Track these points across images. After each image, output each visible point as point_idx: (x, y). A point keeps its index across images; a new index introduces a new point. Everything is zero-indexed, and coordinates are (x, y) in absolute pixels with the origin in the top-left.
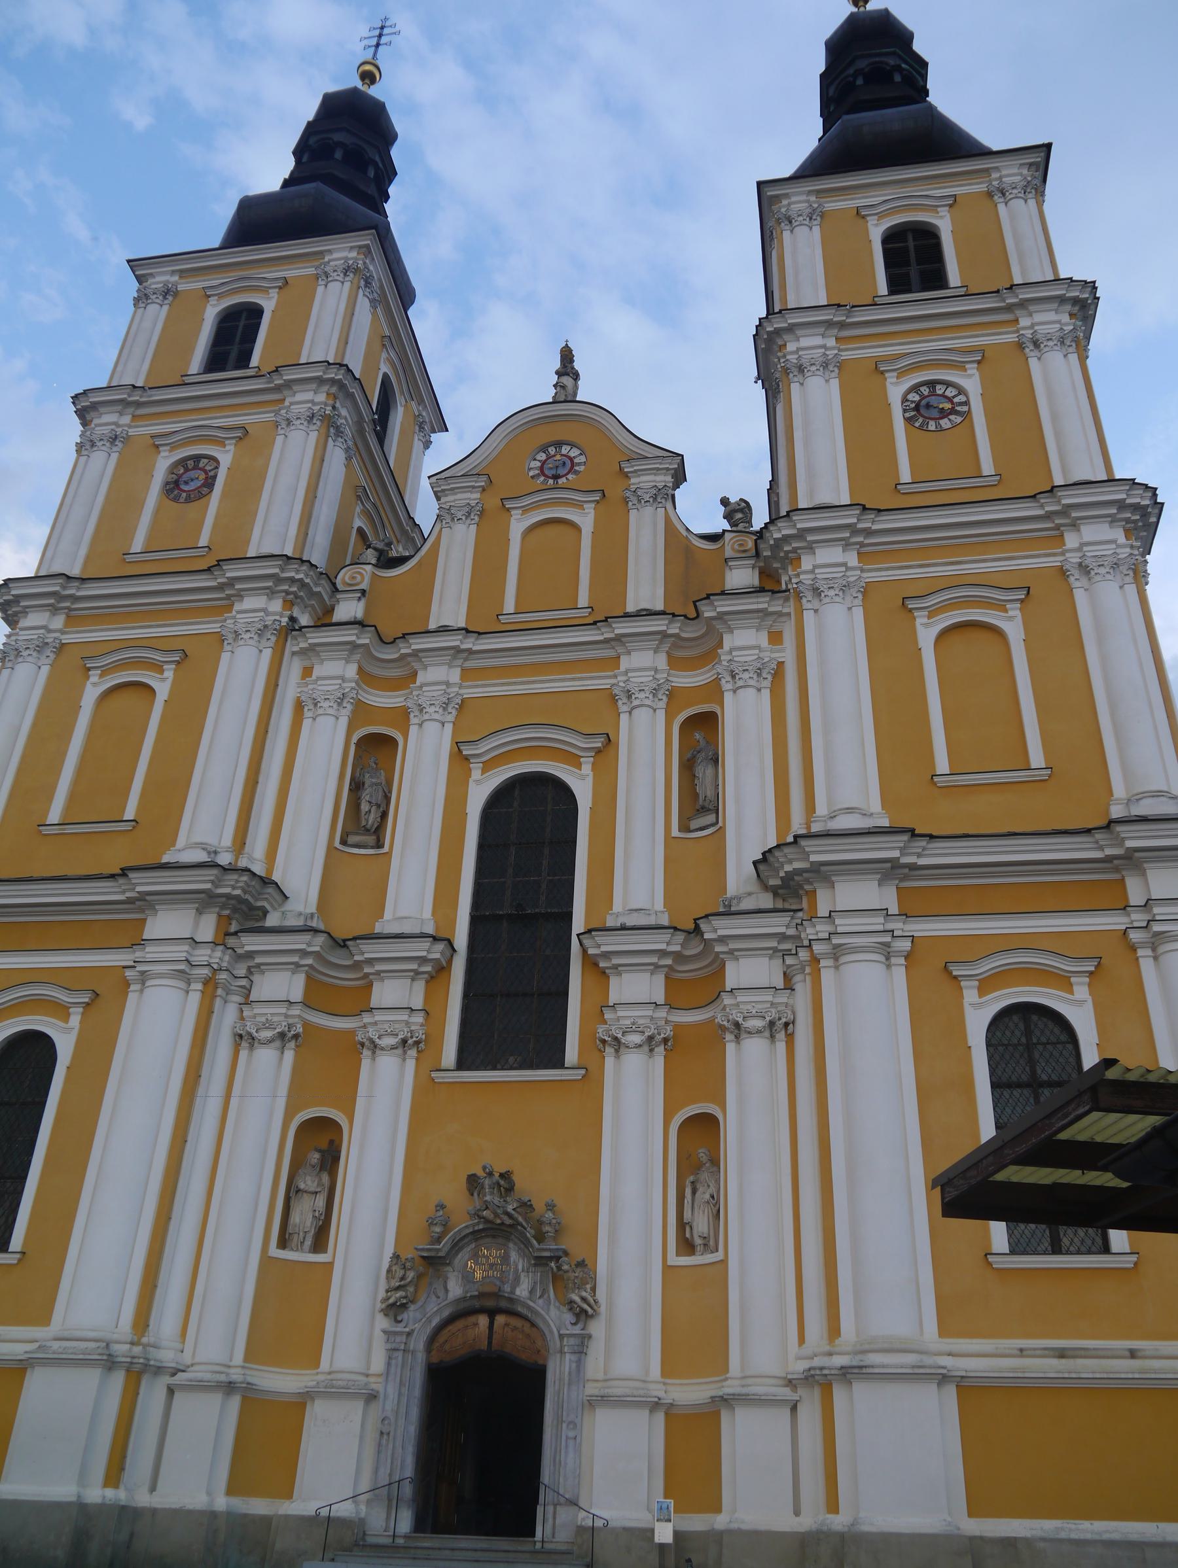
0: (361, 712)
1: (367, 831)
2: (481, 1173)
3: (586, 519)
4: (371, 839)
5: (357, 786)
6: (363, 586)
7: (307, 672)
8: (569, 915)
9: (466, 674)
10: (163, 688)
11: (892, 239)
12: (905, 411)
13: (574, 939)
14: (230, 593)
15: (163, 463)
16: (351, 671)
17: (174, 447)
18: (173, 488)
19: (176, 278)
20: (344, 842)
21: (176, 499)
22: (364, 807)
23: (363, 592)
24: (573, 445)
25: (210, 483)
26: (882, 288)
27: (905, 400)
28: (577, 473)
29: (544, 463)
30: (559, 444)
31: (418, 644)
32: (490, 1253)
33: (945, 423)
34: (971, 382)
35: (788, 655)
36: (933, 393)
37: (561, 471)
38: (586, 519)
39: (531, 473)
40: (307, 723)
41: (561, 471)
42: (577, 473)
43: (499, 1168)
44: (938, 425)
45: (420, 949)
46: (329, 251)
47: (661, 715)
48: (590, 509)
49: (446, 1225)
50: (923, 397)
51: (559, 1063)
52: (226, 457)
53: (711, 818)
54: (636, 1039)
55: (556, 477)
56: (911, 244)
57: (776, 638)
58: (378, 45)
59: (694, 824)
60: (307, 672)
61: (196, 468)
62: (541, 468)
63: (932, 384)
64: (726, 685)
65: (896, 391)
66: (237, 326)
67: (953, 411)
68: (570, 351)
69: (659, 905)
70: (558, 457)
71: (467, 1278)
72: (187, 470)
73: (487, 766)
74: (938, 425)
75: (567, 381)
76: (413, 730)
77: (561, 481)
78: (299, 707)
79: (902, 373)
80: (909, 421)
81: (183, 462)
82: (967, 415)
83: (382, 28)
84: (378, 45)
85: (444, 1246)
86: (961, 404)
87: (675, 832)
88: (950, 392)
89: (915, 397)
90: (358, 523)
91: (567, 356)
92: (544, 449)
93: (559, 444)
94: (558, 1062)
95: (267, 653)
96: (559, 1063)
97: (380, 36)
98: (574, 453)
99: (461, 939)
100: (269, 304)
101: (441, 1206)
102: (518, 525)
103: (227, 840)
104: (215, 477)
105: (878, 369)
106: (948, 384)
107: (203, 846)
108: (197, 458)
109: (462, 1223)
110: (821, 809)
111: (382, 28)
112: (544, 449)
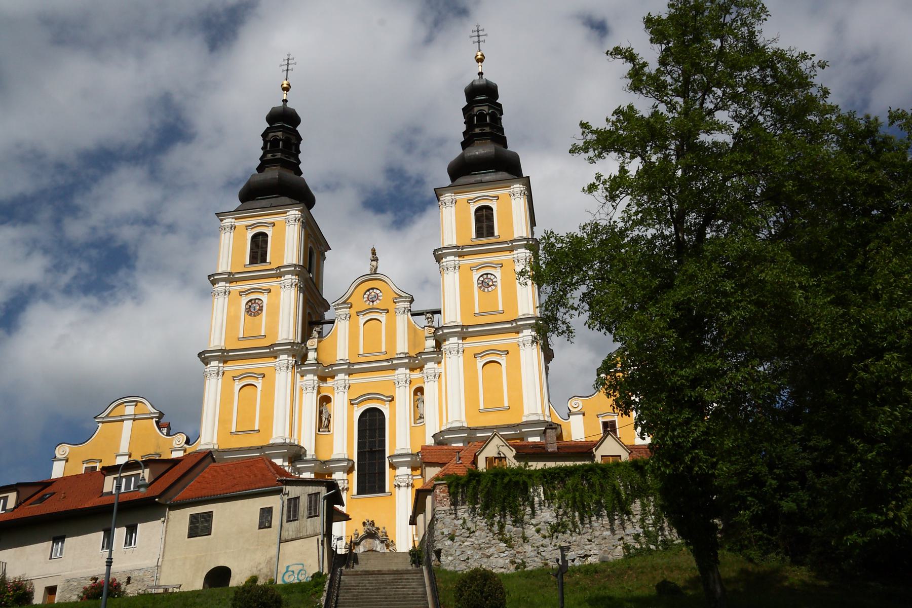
1: (326, 427)
2: (366, 521)
4: (327, 429)
5: (321, 413)
8: (384, 450)
11: (478, 210)
12: (478, 284)
13: (386, 458)
18: (249, 311)
19: (234, 220)
20: (319, 431)
21: (250, 315)
22: (324, 419)
23: (316, 349)
24: (378, 289)
25: (261, 309)
26: (474, 236)
27: (478, 279)
28: (379, 300)
29: (369, 295)
32: (369, 540)
33: (490, 289)
35: (443, 371)
36: (487, 278)
37: (374, 299)
39: (365, 300)
40: (304, 395)
41: (374, 299)
42: (379, 300)
43: (370, 520)
44: (488, 290)
45: (345, 464)
46: (289, 211)
47: (408, 388)
49: (358, 535)
50: (484, 279)
51: (384, 492)
52: (264, 298)
53: (422, 420)
54: (403, 484)
55: (373, 302)
56: (484, 213)
58: (287, 70)
59: (418, 422)
61: (255, 303)
62: (368, 298)
63: (487, 274)
64: (426, 380)
65: (476, 275)
66: (259, 241)
67: (493, 285)
68: (375, 250)
69: (409, 447)
70: (373, 294)
71: (364, 547)
72: (252, 304)
74: (488, 290)
75: (374, 263)
76: (336, 394)
77: (375, 303)
80: (480, 288)
83: (288, 59)
84: (287, 70)
85: (358, 540)
86: (495, 282)
87: (413, 425)
88: (492, 277)
89: (481, 279)
90: (308, 311)
92: (368, 290)
93: (373, 289)
94: (384, 492)
96: (384, 492)
97: (288, 65)
98: (378, 292)
99: (355, 460)
100: (270, 234)
101: (357, 530)
103: (287, 435)
104: (262, 306)
106: (492, 274)
107: (282, 438)
109: (362, 533)
110: (450, 421)
111: (288, 59)
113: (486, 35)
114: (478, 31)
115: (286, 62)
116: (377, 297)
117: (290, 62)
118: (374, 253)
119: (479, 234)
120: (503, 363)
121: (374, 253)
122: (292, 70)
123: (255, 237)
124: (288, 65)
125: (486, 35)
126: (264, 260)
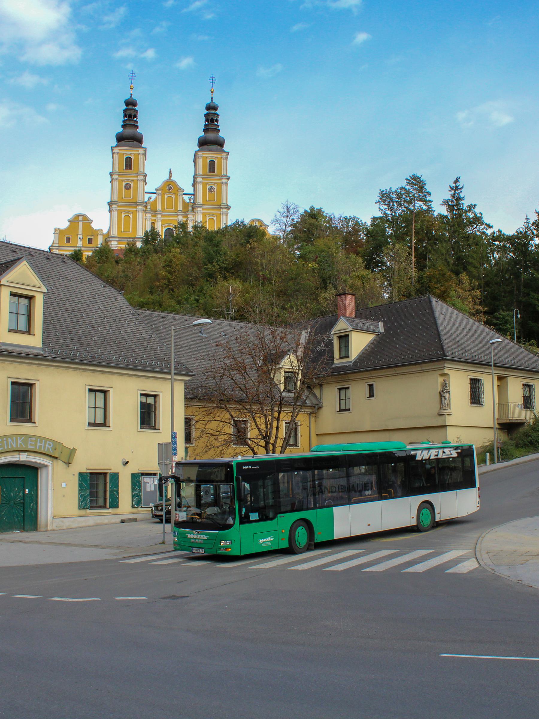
0: (152, 220)
3: (173, 197)
6: (150, 204)
7: (145, 215)
9: (162, 216)
10: (131, 216)
14: (137, 206)
15: (124, 184)
16: (150, 215)
17: (125, 182)
18: (125, 187)
19: (118, 150)
25: (130, 187)
26: (208, 172)
30: (170, 185)
31: (157, 213)
34: (215, 187)
38: (173, 197)
40: (146, 221)
48: (174, 195)
52: (132, 184)
57: (193, 216)
60: (145, 215)
63: (211, 187)
65: (208, 187)
73: (165, 227)
78: (145, 219)
79: (209, 185)
80: (209, 191)
81: (126, 184)
82: (215, 192)
83: (132, 74)
84: (132, 79)
91: (170, 170)
93: (170, 185)
95: (142, 213)
102: (166, 196)
105: (206, 184)
108: (128, 184)
112: (168, 185)
113: (215, 80)
114: (212, 77)
115: (131, 75)
116: (171, 188)
117: (133, 75)
118: (170, 171)
119: (210, 172)
120: (215, 219)
121: (170, 171)
122: (134, 79)
123: (127, 158)
124: (132, 76)
125: (215, 80)
126: (130, 168)
